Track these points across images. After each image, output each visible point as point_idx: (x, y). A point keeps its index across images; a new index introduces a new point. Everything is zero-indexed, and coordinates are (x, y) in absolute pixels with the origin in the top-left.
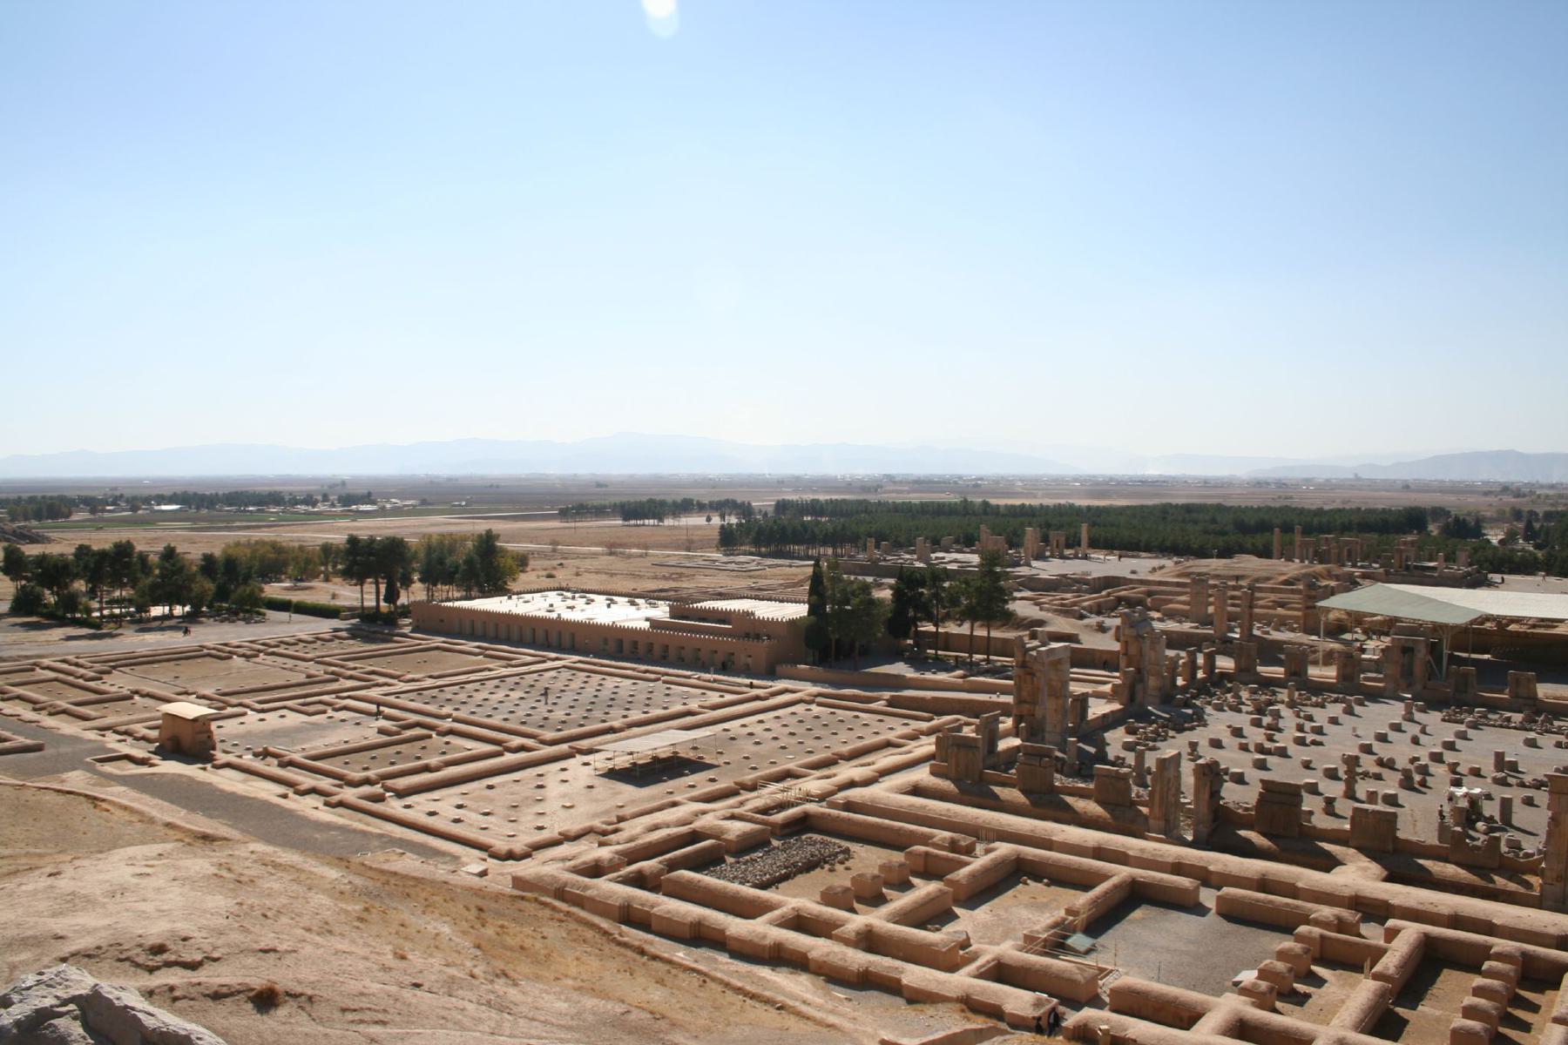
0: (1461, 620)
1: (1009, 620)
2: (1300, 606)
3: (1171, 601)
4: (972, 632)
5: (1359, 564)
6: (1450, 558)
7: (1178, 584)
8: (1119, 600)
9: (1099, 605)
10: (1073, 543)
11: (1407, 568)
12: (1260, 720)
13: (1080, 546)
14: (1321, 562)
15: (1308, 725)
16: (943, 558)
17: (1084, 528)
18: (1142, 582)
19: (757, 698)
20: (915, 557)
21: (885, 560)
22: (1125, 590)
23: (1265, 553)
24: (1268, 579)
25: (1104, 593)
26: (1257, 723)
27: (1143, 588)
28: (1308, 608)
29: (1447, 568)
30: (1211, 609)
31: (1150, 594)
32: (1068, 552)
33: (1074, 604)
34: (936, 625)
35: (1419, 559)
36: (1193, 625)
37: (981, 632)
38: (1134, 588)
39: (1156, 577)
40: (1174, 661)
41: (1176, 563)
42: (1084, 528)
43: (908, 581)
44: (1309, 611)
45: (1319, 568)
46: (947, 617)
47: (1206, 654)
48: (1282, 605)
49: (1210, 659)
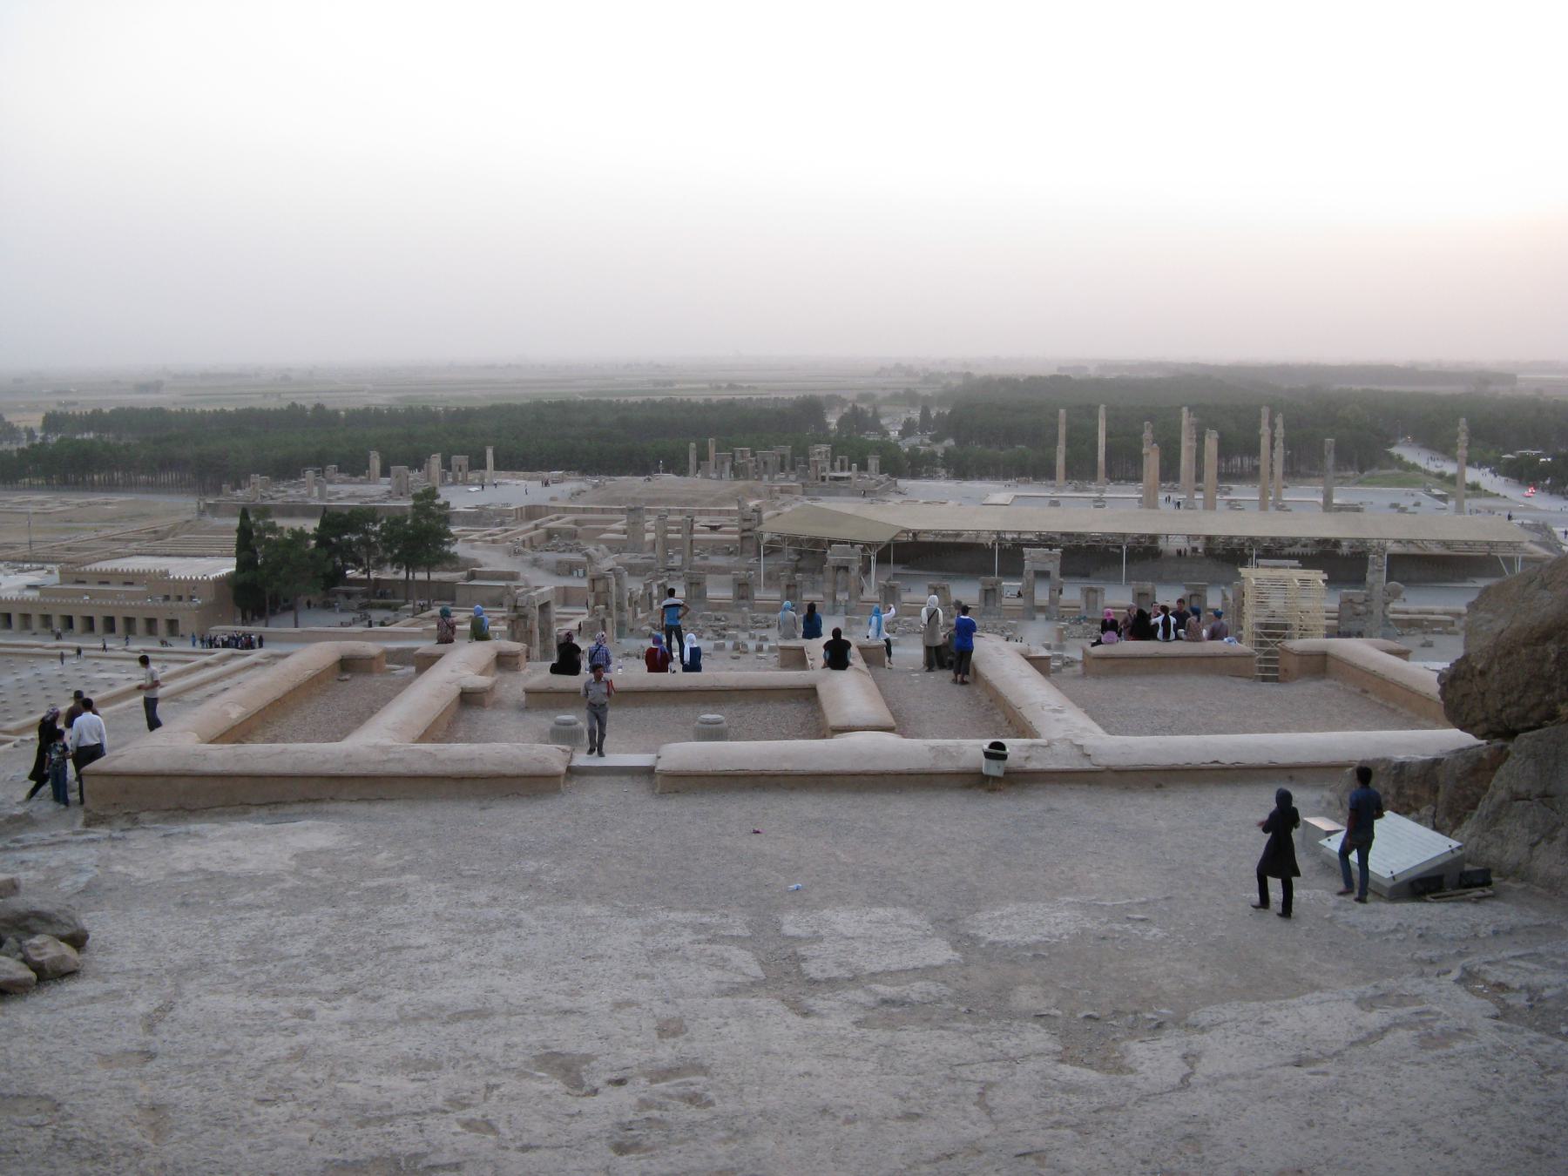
0: (885, 537)
1: (452, 561)
3: (605, 531)
4: (429, 577)
5: (776, 477)
6: (863, 467)
7: (603, 511)
8: (550, 534)
9: (531, 539)
10: (478, 464)
11: (823, 479)
12: (724, 645)
13: (484, 467)
14: (737, 477)
15: (766, 647)
16: (338, 493)
17: (490, 452)
18: (565, 510)
19: (207, 665)
20: (303, 491)
21: (272, 499)
22: (552, 520)
23: (682, 471)
24: (695, 501)
26: (720, 648)
27: (570, 517)
29: (859, 477)
30: (649, 537)
31: (576, 522)
32: (471, 476)
33: (505, 539)
34: (366, 571)
35: (833, 468)
36: (633, 555)
37: (421, 576)
38: (558, 519)
41: (596, 486)
42: (490, 452)
43: (336, 523)
44: (745, 534)
45: (741, 484)
46: (380, 563)
47: (659, 586)
48: (714, 528)
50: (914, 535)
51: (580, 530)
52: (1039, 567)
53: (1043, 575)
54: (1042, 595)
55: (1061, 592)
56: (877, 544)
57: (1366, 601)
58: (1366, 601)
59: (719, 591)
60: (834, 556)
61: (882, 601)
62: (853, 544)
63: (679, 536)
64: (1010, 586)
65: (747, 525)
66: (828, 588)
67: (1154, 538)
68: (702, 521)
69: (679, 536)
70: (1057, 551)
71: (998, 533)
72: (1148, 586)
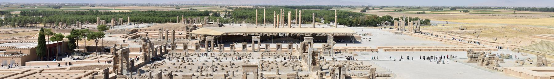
2: (185, 33)
18: (145, 30)
25: (135, 33)
28: (187, 34)
30: (164, 36)
31: (147, 33)
39: (149, 28)
40: (156, 49)
47: (164, 47)
49: (165, 47)
50: (227, 34)
51: (148, 34)
52: (256, 40)
53: (256, 42)
54: (256, 46)
55: (260, 46)
56: (218, 36)
57: (328, 46)
58: (328, 46)
59: (180, 47)
60: (208, 39)
61: (219, 49)
62: (212, 36)
63: (171, 35)
64: (248, 45)
65: (188, 32)
66: (206, 46)
67: (278, 33)
68: (177, 32)
69: (171, 35)
70: (259, 36)
71: (245, 33)
72: (280, 44)
